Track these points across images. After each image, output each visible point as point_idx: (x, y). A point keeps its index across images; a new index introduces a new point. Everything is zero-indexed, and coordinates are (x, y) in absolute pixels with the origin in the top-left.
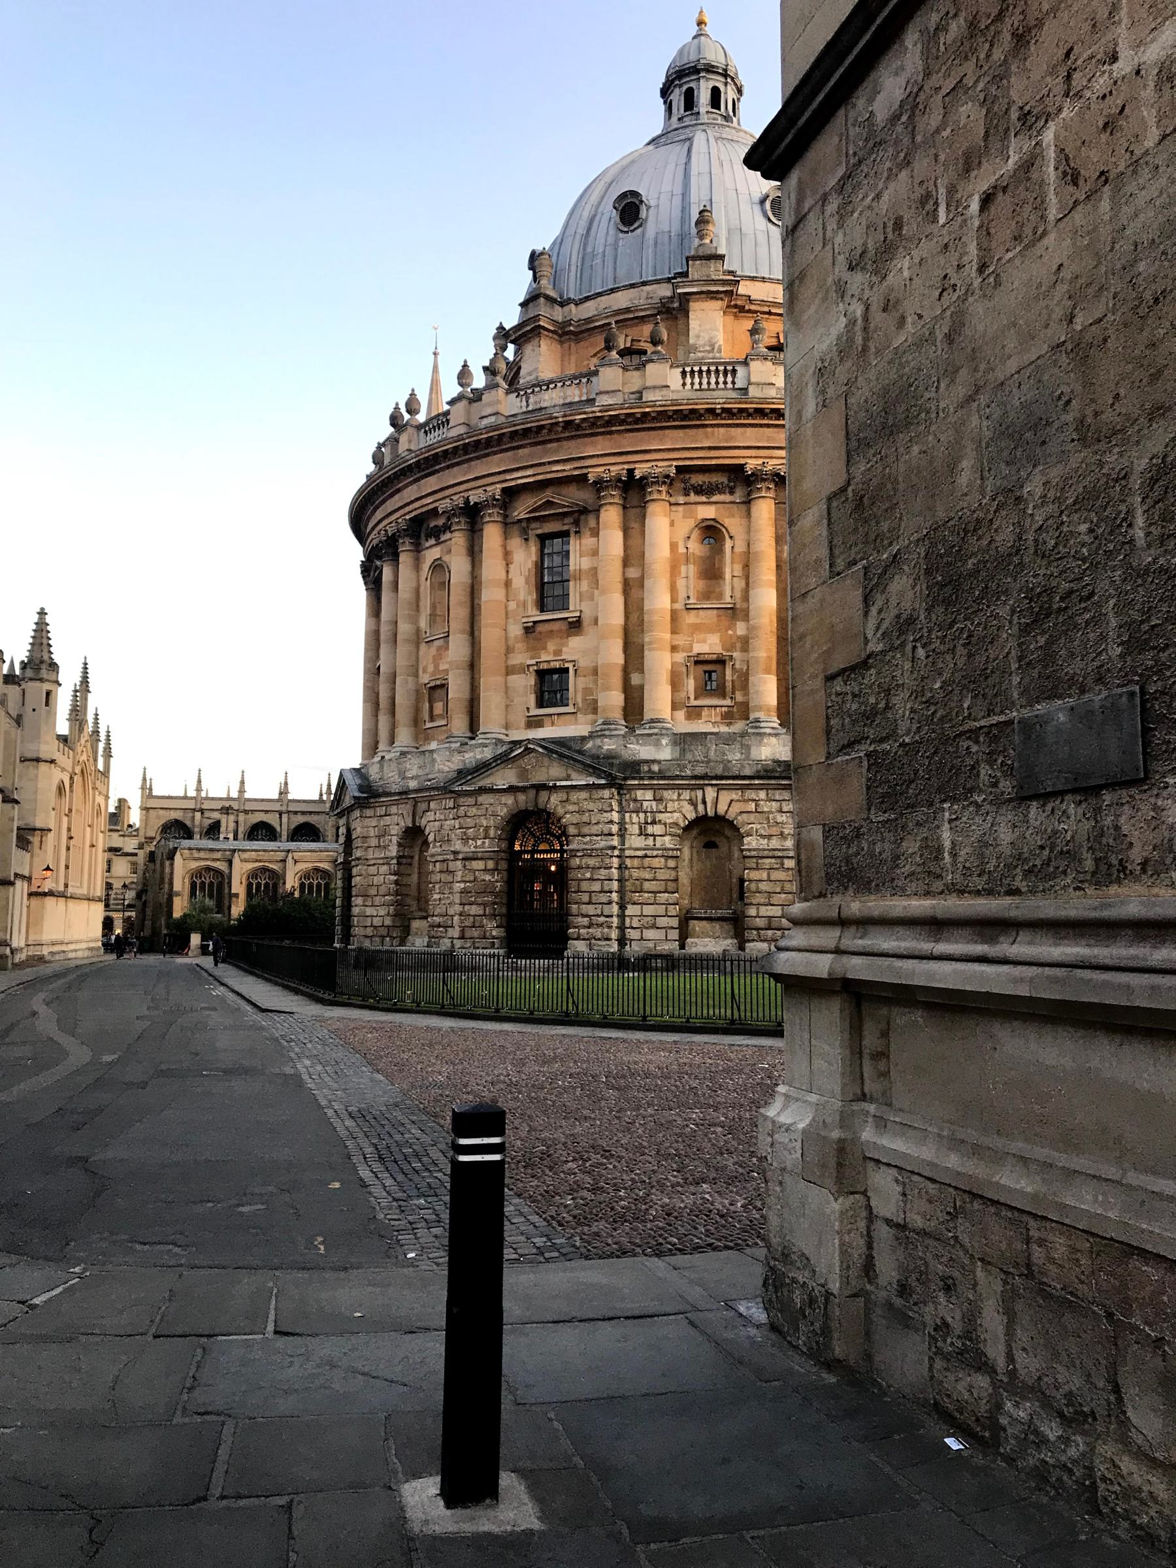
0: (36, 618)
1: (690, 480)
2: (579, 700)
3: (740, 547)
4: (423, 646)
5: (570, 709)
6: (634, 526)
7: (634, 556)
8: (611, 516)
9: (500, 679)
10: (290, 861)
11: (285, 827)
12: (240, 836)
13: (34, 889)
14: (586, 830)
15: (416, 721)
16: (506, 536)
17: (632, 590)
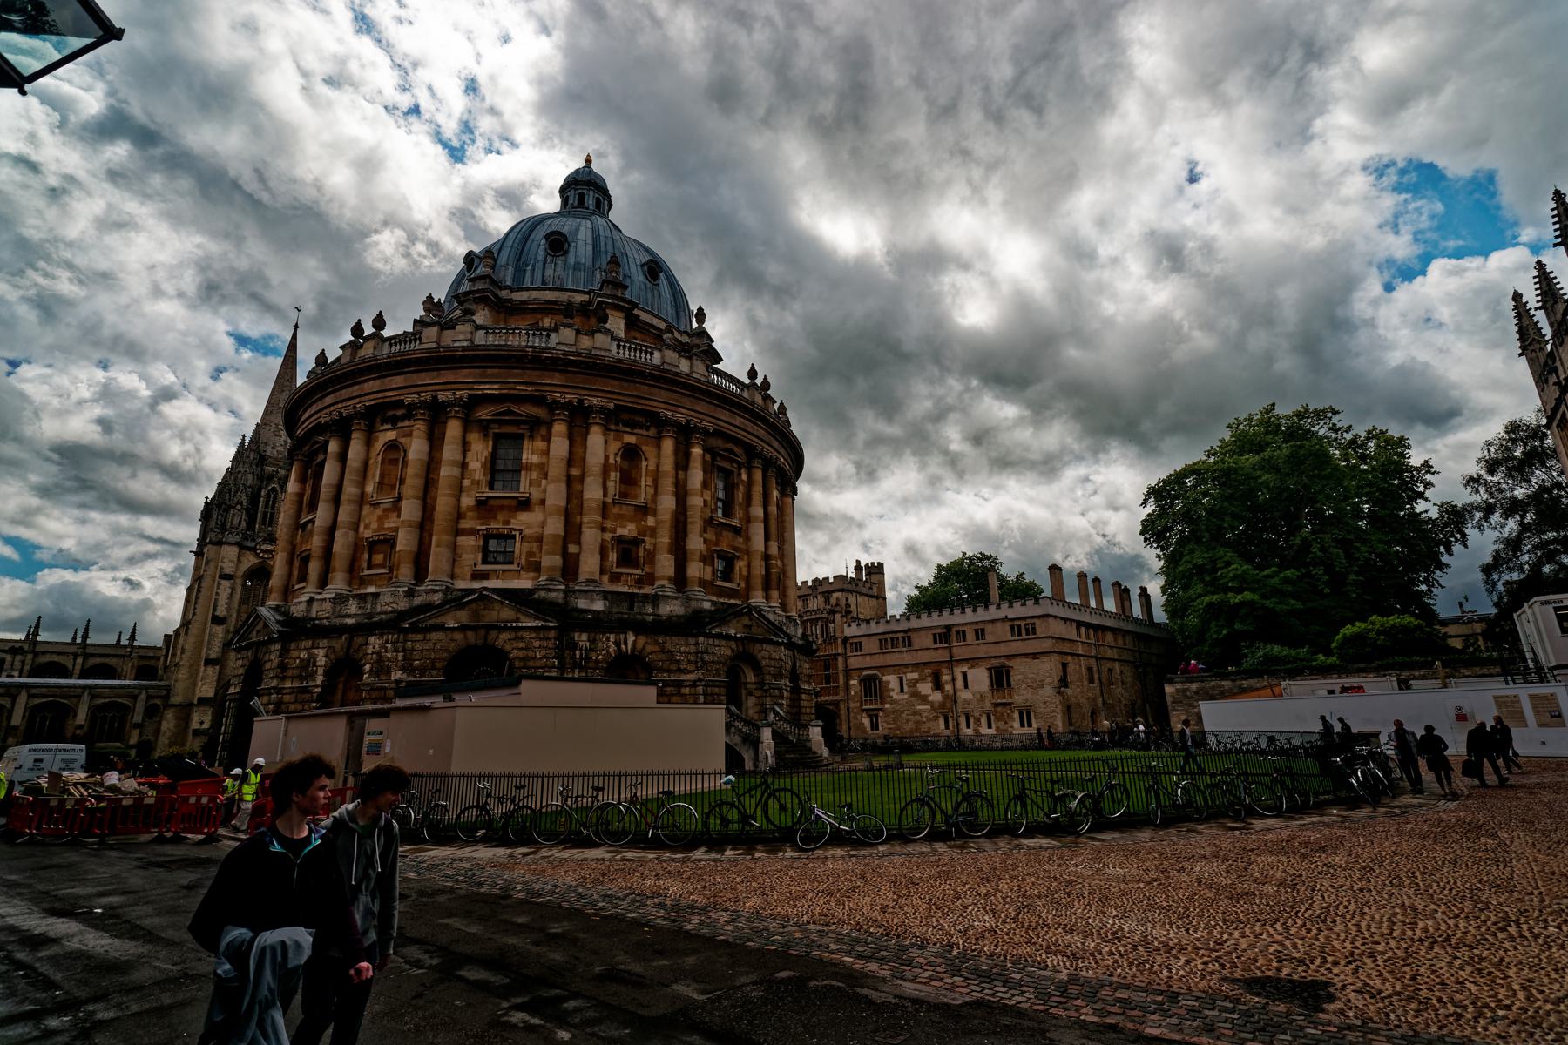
1: (615, 419)
2: (523, 561)
3: (652, 467)
4: (366, 509)
5: (514, 567)
6: (577, 438)
7: (575, 458)
8: (559, 428)
9: (446, 538)
10: (86, 697)
11: (78, 667)
14: (531, 663)
15: (352, 569)
16: (465, 430)
17: (573, 484)
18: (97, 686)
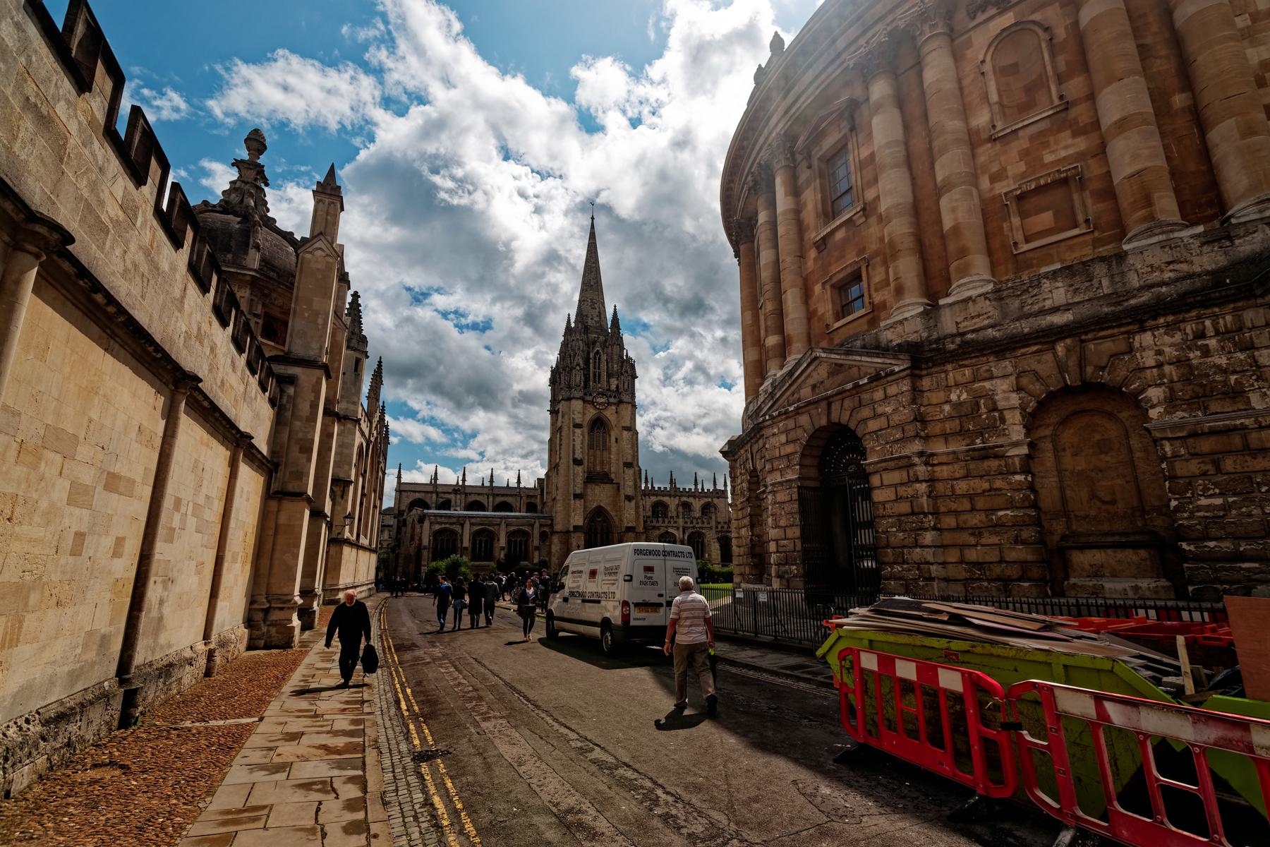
10: (503, 526)
13: (334, 536)
18: (508, 517)
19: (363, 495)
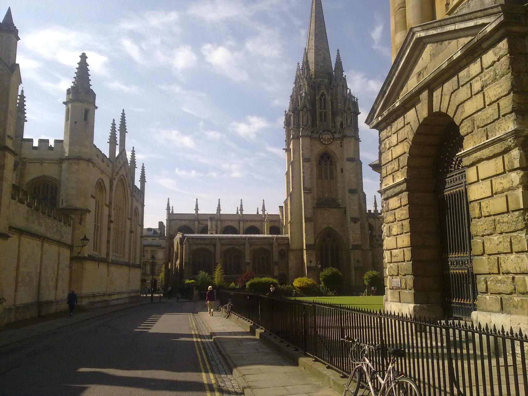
0: (79, 60)
12: (218, 232)
13: (75, 254)
19: (110, 222)
